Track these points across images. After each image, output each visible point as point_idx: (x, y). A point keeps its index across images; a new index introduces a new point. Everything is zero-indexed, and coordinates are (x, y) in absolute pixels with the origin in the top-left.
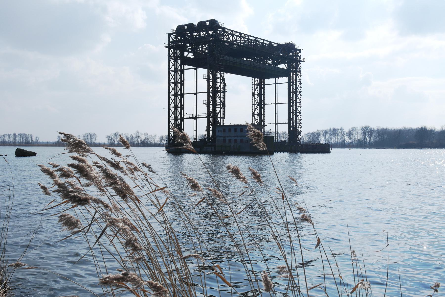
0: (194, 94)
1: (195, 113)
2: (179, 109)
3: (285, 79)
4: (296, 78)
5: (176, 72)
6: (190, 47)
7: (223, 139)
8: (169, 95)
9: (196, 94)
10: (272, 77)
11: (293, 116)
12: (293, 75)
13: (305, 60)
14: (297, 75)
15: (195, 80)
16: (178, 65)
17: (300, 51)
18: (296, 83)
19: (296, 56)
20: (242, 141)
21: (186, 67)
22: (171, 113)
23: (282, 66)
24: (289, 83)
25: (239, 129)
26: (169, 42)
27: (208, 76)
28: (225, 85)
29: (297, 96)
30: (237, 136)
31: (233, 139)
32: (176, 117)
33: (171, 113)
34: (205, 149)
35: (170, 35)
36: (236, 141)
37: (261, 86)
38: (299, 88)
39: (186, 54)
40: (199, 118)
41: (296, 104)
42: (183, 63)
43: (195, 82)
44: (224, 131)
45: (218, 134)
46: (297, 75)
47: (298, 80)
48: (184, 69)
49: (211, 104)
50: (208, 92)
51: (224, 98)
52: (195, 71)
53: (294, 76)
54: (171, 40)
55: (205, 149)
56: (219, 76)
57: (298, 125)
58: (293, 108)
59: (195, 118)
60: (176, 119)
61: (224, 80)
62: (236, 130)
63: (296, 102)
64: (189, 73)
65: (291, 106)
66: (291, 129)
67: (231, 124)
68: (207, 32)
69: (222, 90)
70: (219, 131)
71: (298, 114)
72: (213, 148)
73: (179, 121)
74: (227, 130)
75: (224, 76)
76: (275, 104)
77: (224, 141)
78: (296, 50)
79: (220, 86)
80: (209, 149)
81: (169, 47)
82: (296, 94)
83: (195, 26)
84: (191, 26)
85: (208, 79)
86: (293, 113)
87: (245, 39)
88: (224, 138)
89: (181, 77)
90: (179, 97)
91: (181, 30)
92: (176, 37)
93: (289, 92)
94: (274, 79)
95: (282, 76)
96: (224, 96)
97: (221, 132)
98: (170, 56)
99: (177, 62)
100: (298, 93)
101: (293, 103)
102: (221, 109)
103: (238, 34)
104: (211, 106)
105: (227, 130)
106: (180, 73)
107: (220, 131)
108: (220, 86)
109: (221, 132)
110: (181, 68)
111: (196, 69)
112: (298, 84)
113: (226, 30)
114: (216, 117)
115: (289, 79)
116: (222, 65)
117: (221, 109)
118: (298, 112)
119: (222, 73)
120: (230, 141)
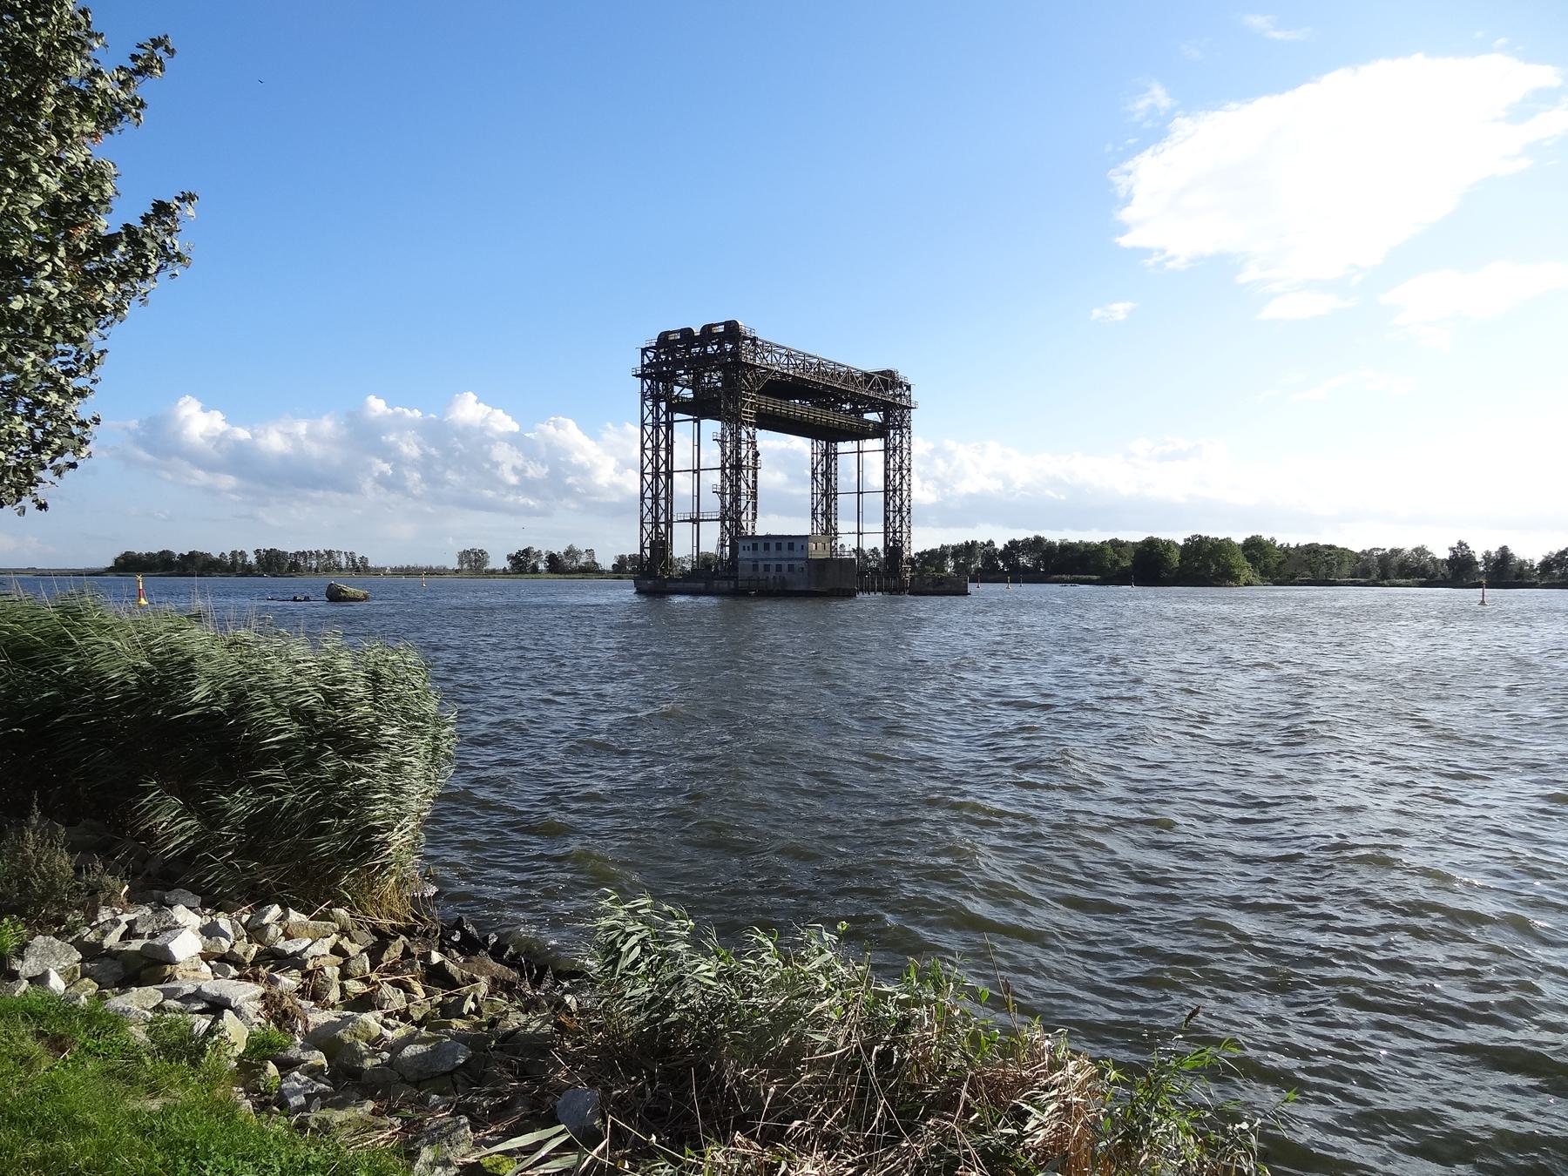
0: (694, 471)
1: (695, 511)
2: (662, 503)
3: (878, 443)
4: (901, 442)
5: (656, 427)
6: (686, 377)
8: (642, 474)
9: (697, 471)
11: (895, 517)
12: (895, 434)
13: (920, 406)
14: (902, 436)
15: (696, 443)
16: (661, 413)
17: (909, 388)
18: (901, 452)
19: (900, 395)
20: (791, 568)
21: (678, 416)
22: (646, 510)
23: (869, 416)
24: (886, 450)
25: (785, 545)
26: (643, 366)
27: (723, 435)
28: (756, 454)
29: (902, 477)
30: (782, 559)
31: (773, 564)
32: (656, 518)
33: (646, 510)
35: (644, 351)
36: (779, 568)
37: (830, 456)
38: (906, 462)
39: (677, 389)
40: (703, 520)
41: (901, 494)
42: (672, 408)
43: (696, 448)
44: (755, 547)
45: (742, 554)
46: (902, 436)
47: (905, 446)
48: (673, 421)
49: (728, 492)
50: (723, 468)
51: (755, 482)
52: (696, 424)
53: (898, 436)
54: (646, 361)
56: (744, 435)
57: (905, 535)
58: (894, 502)
59: (696, 521)
60: (656, 524)
61: (754, 444)
63: (901, 490)
64: (683, 430)
65: (890, 498)
66: (891, 544)
68: (720, 345)
69: (750, 464)
71: (904, 514)
72: (732, 582)
73: (663, 526)
74: (761, 546)
75: (754, 436)
76: (859, 493)
77: (755, 567)
78: (901, 385)
79: (747, 456)
80: (725, 585)
81: (643, 376)
82: (901, 474)
84: (686, 333)
85: (722, 442)
86: (895, 512)
87: (798, 362)
89: (666, 437)
90: (663, 477)
91: (664, 338)
92: (657, 356)
93: (886, 469)
94: (855, 443)
95: (873, 438)
96: (755, 475)
98: (643, 395)
99: (658, 407)
100: (905, 472)
101: (895, 491)
102: (748, 502)
103: (783, 351)
104: (728, 497)
105: (761, 546)
106: (664, 429)
108: (747, 456)
110: (667, 418)
111: (697, 421)
112: (905, 454)
113: (760, 343)
114: (738, 520)
115: (886, 444)
116: (751, 413)
117: (748, 502)
118: (905, 509)
119: (750, 429)
120: (767, 568)
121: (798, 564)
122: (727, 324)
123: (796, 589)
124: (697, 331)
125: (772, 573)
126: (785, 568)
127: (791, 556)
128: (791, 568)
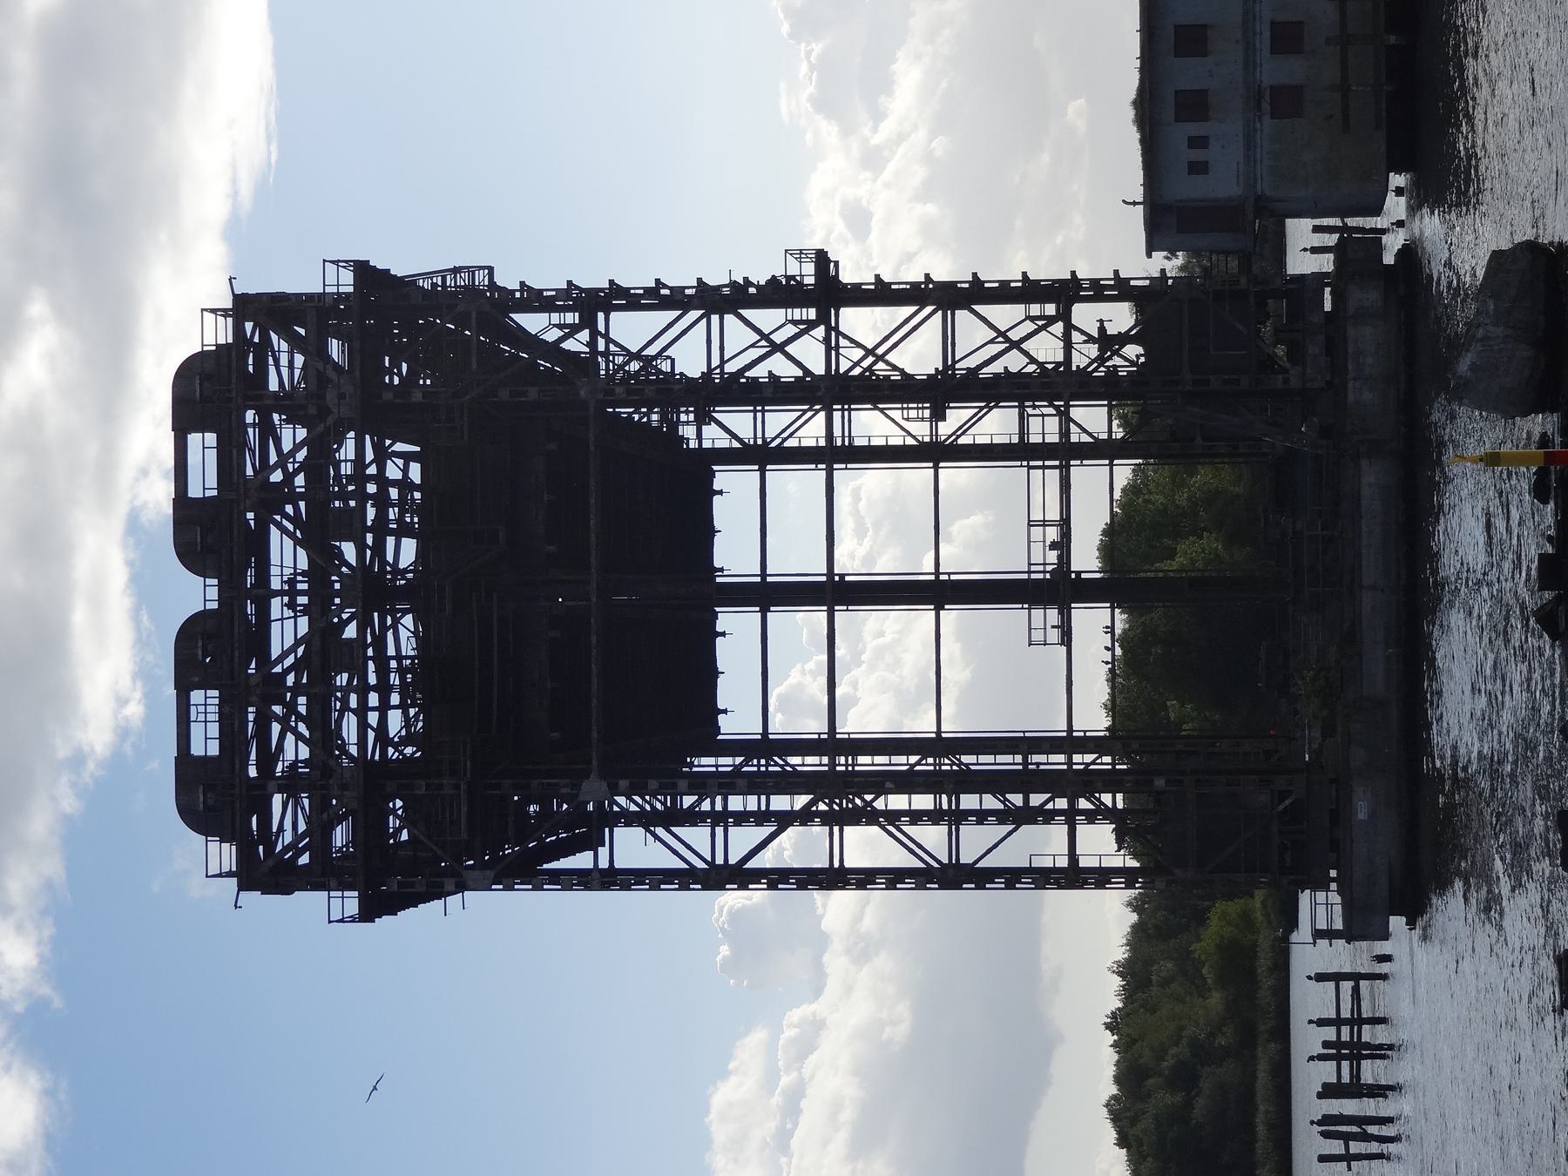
7: (1267, 120)
8: (835, 878)
34: (1367, 396)
45: (1223, 183)
55: (1367, 396)
62: (1194, 105)
67: (1138, 194)
70: (1199, 168)
77: (1286, 102)
88: (1266, 106)
105: (1189, 74)
107: (1197, 155)
109: (1198, 142)
122: (186, 417)
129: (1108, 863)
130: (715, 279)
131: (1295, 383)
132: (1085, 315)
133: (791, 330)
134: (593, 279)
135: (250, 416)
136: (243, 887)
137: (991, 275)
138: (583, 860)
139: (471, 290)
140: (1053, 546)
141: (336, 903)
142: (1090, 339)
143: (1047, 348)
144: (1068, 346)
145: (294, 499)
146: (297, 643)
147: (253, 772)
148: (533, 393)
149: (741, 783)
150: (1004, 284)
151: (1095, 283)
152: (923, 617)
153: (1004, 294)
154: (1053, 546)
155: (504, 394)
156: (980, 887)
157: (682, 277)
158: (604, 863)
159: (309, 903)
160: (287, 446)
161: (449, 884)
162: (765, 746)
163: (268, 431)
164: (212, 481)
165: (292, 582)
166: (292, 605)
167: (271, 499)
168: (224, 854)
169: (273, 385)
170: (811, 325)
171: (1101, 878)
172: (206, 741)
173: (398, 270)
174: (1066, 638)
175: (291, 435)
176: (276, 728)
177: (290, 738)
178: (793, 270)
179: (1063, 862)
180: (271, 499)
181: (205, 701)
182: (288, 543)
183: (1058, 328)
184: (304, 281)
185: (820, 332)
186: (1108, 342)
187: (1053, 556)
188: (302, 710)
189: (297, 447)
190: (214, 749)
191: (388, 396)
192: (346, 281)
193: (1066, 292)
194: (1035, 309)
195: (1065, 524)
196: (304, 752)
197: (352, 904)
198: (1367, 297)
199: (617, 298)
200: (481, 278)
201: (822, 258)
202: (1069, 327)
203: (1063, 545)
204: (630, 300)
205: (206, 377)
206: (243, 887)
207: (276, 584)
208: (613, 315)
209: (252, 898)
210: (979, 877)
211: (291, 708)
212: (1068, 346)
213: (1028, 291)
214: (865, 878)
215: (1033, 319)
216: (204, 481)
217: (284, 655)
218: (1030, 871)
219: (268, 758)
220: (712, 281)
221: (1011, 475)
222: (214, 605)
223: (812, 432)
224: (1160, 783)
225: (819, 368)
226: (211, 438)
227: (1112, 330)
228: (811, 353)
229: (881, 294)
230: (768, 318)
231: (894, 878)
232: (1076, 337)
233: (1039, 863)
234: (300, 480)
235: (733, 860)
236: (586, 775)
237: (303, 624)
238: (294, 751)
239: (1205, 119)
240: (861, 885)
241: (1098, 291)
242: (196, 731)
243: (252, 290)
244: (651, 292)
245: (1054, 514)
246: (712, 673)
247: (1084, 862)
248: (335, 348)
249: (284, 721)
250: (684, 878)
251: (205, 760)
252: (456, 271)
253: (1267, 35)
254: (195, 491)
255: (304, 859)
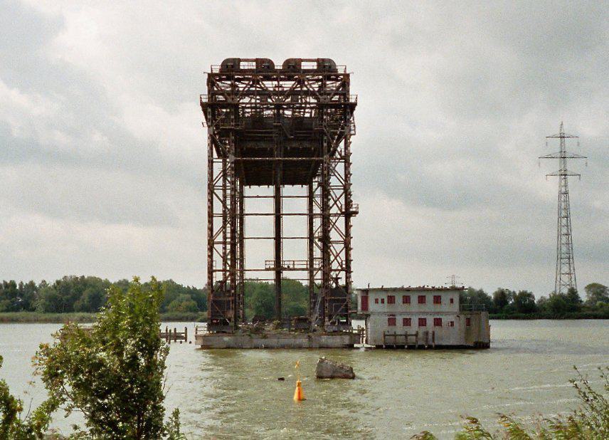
8: (211, 215)
10: (269, 184)
20: (438, 322)
30: (427, 313)
36: (422, 322)
45: (372, 306)
70: (377, 301)
74: (399, 299)
83: (276, 68)
91: (230, 69)
97: (383, 301)
105: (399, 299)
120: (407, 322)
121: (446, 320)
122: (321, 62)
123: (444, 344)
124: (279, 65)
125: (414, 327)
126: (430, 321)
127: (438, 310)
128: (438, 322)
129: (214, 279)
130: (352, 188)
131: (326, 323)
132: (343, 274)
133: (340, 205)
134: (352, 159)
135: (321, 77)
136: (209, 74)
137: (352, 252)
138: (215, 155)
139: (350, 130)
140: (289, 267)
141: (205, 97)
142: (337, 275)
143: (335, 265)
144: (335, 270)
145: (301, 87)
146: (267, 88)
147: (236, 77)
148: (325, 144)
149: (233, 193)
150: (350, 255)
151: (350, 277)
152: (273, 236)
153: (347, 255)
154: (289, 267)
155: (325, 138)
156: (208, 249)
157: (352, 179)
158: (214, 160)
159: (205, 90)
160: (313, 86)
161: (210, 124)
162: (242, 197)
163: (318, 80)
164: (305, 68)
165: (281, 87)
166: (276, 87)
167: (300, 82)
168: (216, 71)
169: (328, 82)
170: (341, 210)
171: (211, 277)
172: (243, 66)
173: (355, 112)
174: (267, 270)
175: (316, 86)
176: (247, 82)
177: (245, 85)
178: (354, 206)
179: (214, 268)
180: (300, 82)
181: (253, 66)
182: (291, 86)
183: (340, 268)
184: (354, 91)
185: (339, 212)
186: (336, 279)
187: (286, 266)
188: (251, 89)
189: (313, 88)
190: (241, 68)
191: (325, 110)
192: (352, 101)
193: (348, 270)
194: (344, 263)
195: (294, 269)
196: (241, 89)
197: (204, 101)
198: (347, 340)
199: (348, 165)
200: (352, 132)
201: (356, 213)
202: (340, 271)
203: (289, 269)
204: (347, 168)
205: (330, 67)
206: (209, 74)
207: (281, 83)
208: (343, 164)
209: (206, 76)
210: (211, 249)
211: (252, 86)
212: (335, 270)
213: (348, 261)
214: (211, 222)
215: (342, 261)
216: (305, 66)
217: (264, 85)
218: (212, 261)
219: (239, 80)
220: (351, 187)
221: (306, 258)
222: (276, 68)
223: (317, 210)
224: (233, 291)
225: (331, 212)
226: (315, 68)
227: (339, 280)
228: (334, 210)
229: (348, 227)
230: (342, 200)
231: (211, 229)
232: (337, 272)
233: (214, 263)
234: (305, 89)
235: (215, 191)
236: (235, 156)
237: (272, 89)
238: (241, 86)
239: (388, 303)
240: (209, 221)
241: (348, 277)
242: (246, 63)
243: (350, 78)
244: (349, 173)
245: (296, 267)
246: (259, 184)
247: (214, 274)
248: (336, 98)
249: (248, 84)
250: (211, 179)
251: (239, 65)
252: (354, 126)
253: (408, 317)
254: (303, 63)
255: (215, 89)
